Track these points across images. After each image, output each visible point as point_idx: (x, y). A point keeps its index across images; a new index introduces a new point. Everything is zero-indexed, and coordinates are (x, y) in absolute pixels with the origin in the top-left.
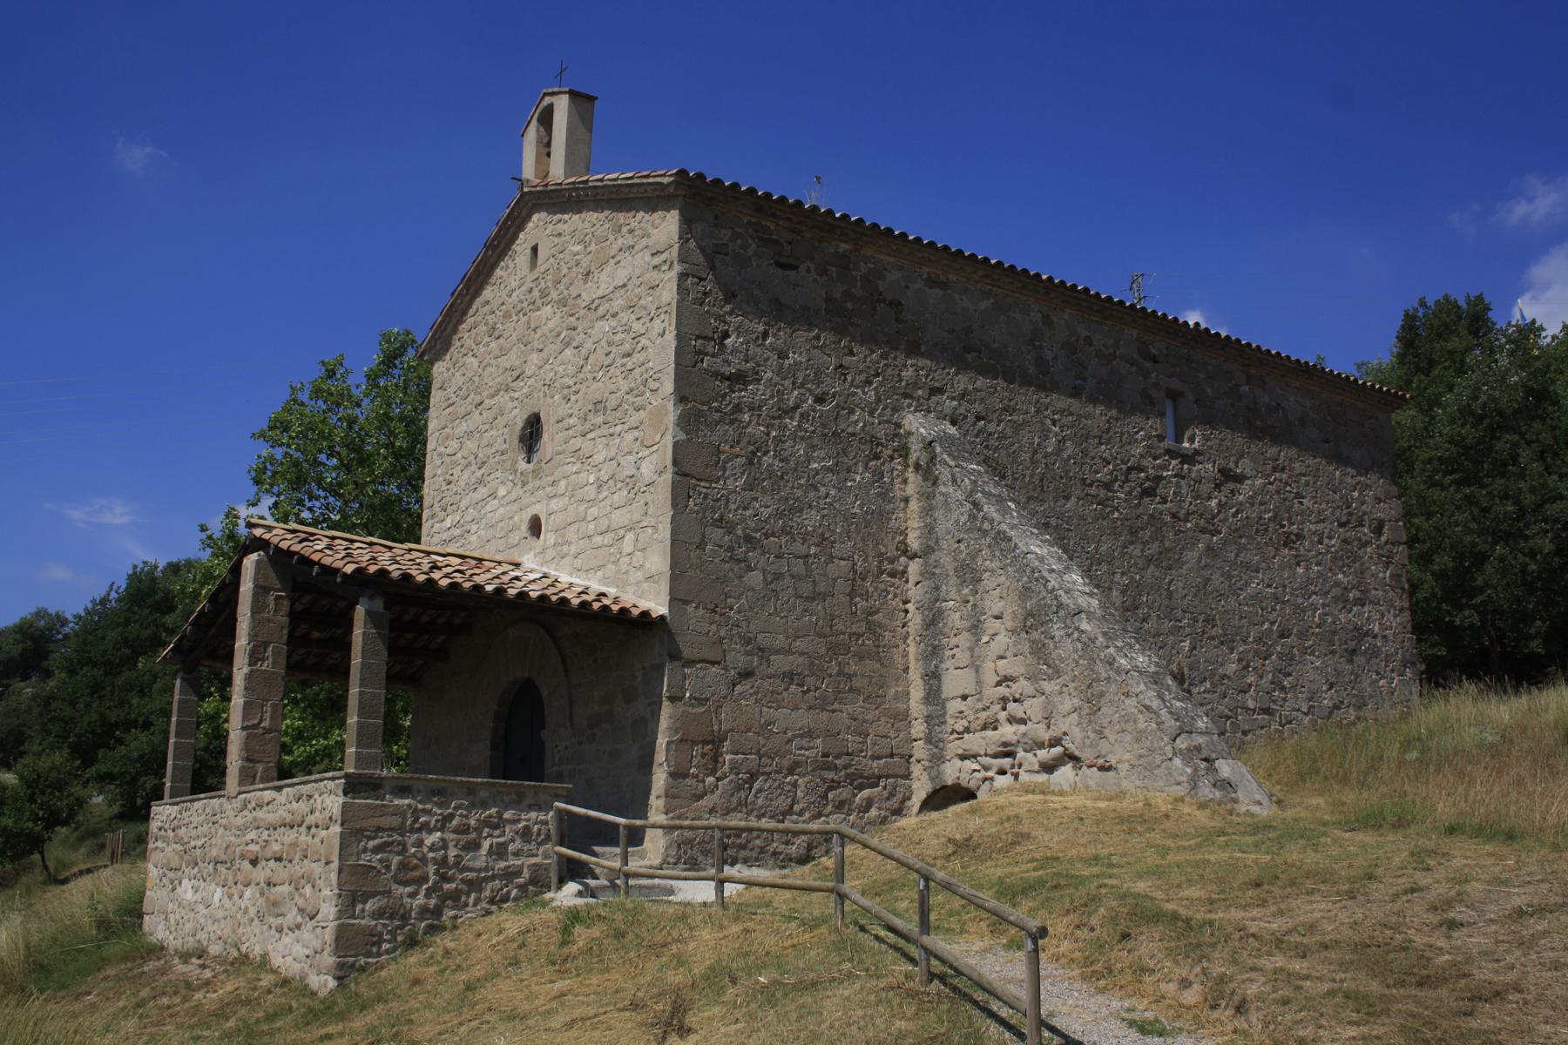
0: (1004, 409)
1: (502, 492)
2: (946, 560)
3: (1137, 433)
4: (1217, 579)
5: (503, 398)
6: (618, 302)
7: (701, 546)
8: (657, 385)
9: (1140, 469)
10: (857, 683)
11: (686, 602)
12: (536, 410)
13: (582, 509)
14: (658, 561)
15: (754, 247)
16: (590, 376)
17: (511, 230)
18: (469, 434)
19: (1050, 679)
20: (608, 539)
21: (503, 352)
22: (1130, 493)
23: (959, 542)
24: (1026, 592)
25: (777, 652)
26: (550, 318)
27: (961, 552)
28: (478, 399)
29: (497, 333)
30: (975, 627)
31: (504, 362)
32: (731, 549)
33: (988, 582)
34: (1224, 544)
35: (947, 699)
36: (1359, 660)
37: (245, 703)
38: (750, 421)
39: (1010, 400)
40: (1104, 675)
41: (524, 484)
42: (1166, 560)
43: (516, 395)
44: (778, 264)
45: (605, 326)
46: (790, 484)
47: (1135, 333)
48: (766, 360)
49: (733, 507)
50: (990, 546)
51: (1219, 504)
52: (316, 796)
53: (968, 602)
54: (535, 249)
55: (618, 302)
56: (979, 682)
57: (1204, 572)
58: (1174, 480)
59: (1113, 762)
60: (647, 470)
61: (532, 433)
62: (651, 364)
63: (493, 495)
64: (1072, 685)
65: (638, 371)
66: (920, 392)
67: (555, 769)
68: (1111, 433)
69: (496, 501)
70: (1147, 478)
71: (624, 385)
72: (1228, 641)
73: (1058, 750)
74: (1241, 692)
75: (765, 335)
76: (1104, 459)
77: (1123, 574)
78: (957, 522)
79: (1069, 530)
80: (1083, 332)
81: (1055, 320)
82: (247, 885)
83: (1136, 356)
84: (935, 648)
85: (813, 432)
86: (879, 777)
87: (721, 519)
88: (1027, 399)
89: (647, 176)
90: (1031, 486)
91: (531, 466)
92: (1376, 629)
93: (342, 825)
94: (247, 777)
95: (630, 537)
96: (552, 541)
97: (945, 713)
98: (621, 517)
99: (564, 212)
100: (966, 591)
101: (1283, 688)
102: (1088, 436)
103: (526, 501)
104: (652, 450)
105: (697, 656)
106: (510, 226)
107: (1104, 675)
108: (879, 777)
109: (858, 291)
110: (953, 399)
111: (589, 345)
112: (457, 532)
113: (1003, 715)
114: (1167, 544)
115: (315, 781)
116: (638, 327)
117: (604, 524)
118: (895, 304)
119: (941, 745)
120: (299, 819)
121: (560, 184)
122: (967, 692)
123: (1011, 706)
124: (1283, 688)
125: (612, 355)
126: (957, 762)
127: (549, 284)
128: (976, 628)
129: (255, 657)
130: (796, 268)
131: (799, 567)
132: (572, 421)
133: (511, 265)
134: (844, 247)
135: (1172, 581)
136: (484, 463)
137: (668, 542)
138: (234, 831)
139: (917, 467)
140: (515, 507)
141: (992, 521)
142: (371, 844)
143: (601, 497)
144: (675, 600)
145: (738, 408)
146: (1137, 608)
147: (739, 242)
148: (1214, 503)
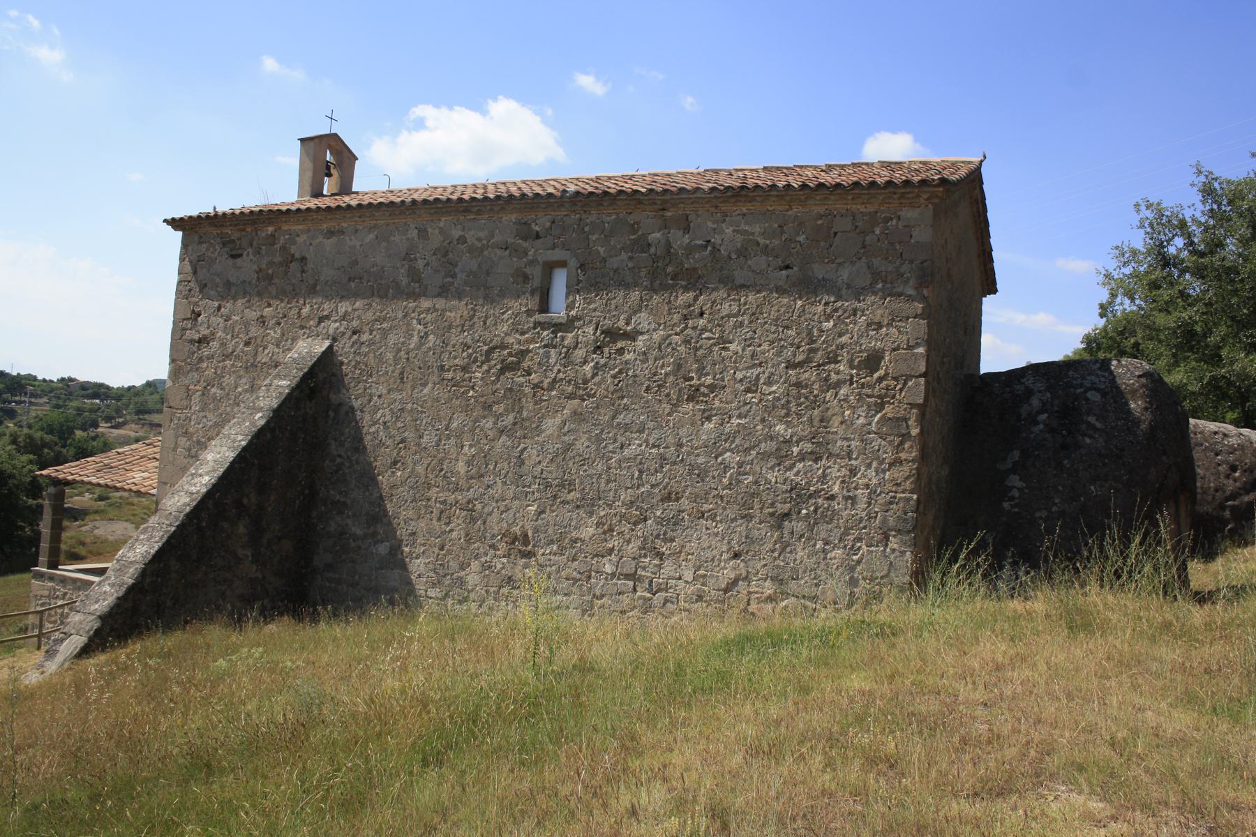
0: (376, 320)
3: (503, 313)
4: (582, 444)
7: (175, 449)
9: (502, 346)
11: (165, 484)
22: (488, 371)
32: (189, 450)
34: (597, 407)
38: (208, 366)
39: (381, 312)
42: (522, 428)
46: (224, 404)
47: (513, 217)
48: (218, 324)
49: (193, 423)
51: (596, 367)
57: (566, 438)
58: (541, 351)
66: (311, 323)
68: (475, 319)
70: (510, 354)
72: (587, 504)
74: (597, 555)
75: (219, 308)
76: (465, 345)
77: (471, 446)
79: (422, 412)
80: (456, 233)
85: (241, 367)
87: (186, 433)
90: (392, 380)
92: (836, 488)
101: (660, 555)
102: (450, 327)
110: (336, 321)
114: (525, 414)
118: (303, 259)
124: (660, 555)
134: (271, 229)
135: (525, 448)
142: (40, 602)
145: (201, 360)
146: (482, 476)
148: (588, 368)
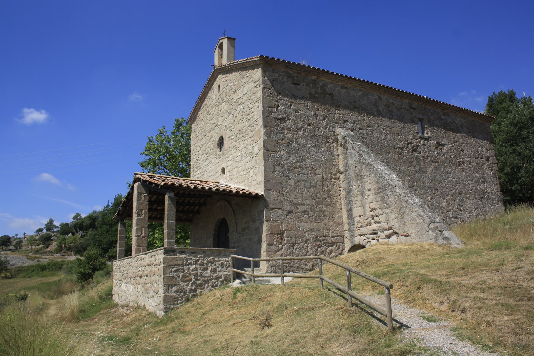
0: (368, 126)
1: (213, 161)
2: (352, 173)
3: (410, 132)
4: (438, 177)
5: (212, 132)
6: (245, 99)
7: (274, 172)
8: (257, 123)
9: (412, 143)
10: (326, 213)
11: (270, 190)
12: (222, 135)
13: (237, 164)
14: (261, 178)
15: (286, 78)
16: (237, 123)
17: (212, 81)
18: (203, 145)
19: (387, 208)
20: (245, 172)
21: (212, 119)
22: (409, 151)
23: (356, 167)
24: (378, 181)
25: (300, 205)
26: (224, 106)
27: (356, 170)
28: (205, 134)
29: (209, 113)
30: (362, 193)
31: (212, 122)
32: (283, 173)
33: (366, 179)
34: (440, 166)
35: (354, 217)
36: (484, 200)
37: (136, 228)
38: (287, 133)
39: (369, 123)
40: (405, 206)
41: (219, 158)
42: (422, 171)
43: (216, 131)
44: (294, 84)
45: (241, 107)
46: (301, 152)
47: (407, 101)
48: (291, 113)
49: (283, 160)
50: (365, 168)
51: (437, 153)
52: (156, 256)
53: (360, 186)
54: (219, 86)
55: (245, 99)
56: (364, 211)
57: (434, 175)
58: (423, 146)
59: (409, 234)
60: (256, 150)
61: (221, 142)
62: (255, 117)
63: (210, 162)
64: (394, 210)
65: (251, 119)
66: (341, 122)
67: (233, 245)
68: (402, 132)
69: (212, 164)
70: (414, 146)
71: (248, 124)
72: (442, 196)
73: (391, 231)
74: (448, 212)
75: (291, 106)
76: (400, 140)
77: (408, 176)
78: (355, 161)
79: (390, 163)
80: (391, 101)
81: (382, 98)
82: (139, 284)
83: (408, 108)
84: (350, 201)
85: (308, 135)
86: (334, 243)
87: (280, 164)
88: (375, 121)
89: (251, 59)
90: (378, 150)
91: (221, 152)
92: (489, 191)
93: (164, 264)
94: (138, 251)
95: (252, 171)
96: (229, 175)
97: (354, 222)
98: (249, 165)
99: (227, 74)
100: (359, 183)
101: (461, 210)
102: (395, 134)
103: (220, 163)
104: (257, 143)
105: (274, 207)
106: (212, 80)
107: (405, 206)
108: (334, 243)
109: (319, 91)
110: (351, 123)
111: (236, 113)
112: (200, 175)
113: (373, 221)
114: (422, 166)
115: (156, 251)
116: (251, 106)
117: (243, 168)
118: (331, 95)
119: (353, 232)
120: (152, 263)
121: (225, 65)
122: (361, 214)
123: (375, 218)
124: (461, 210)
125: (243, 116)
126: (359, 237)
127: (224, 96)
128: (362, 194)
129: (139, 214)
130: (299, 84)
131: (305, 178)
132: (232, 137)
133: (212, 92)
134: (314, 77)
135: (424, 178)
136: (207, 153)
137: (263, 171)
138: (135, 268)
139: (341, 145)
140: (217, 165)
141: (366, 160)
142: (173, 270)
143: (242, 160)
144: (267, 189)
145: (283, 129)
146: (413, 187)
147: (281, 77)
148: (435, 153)
